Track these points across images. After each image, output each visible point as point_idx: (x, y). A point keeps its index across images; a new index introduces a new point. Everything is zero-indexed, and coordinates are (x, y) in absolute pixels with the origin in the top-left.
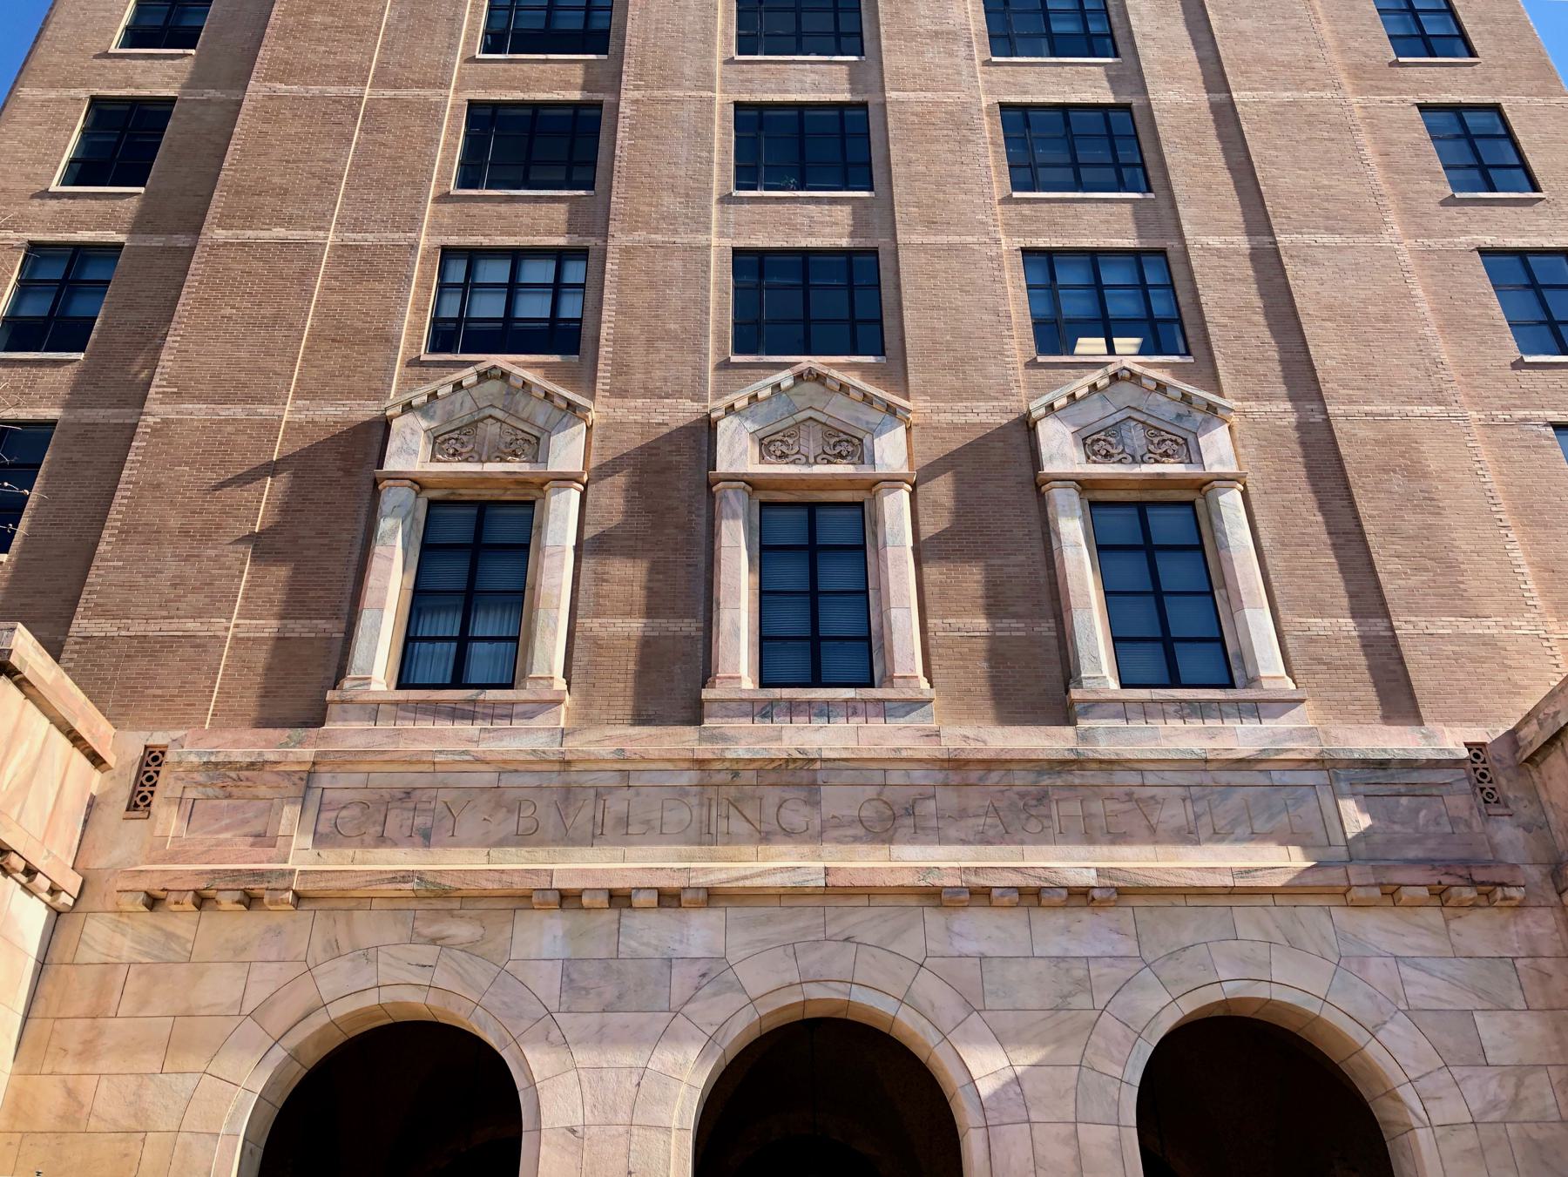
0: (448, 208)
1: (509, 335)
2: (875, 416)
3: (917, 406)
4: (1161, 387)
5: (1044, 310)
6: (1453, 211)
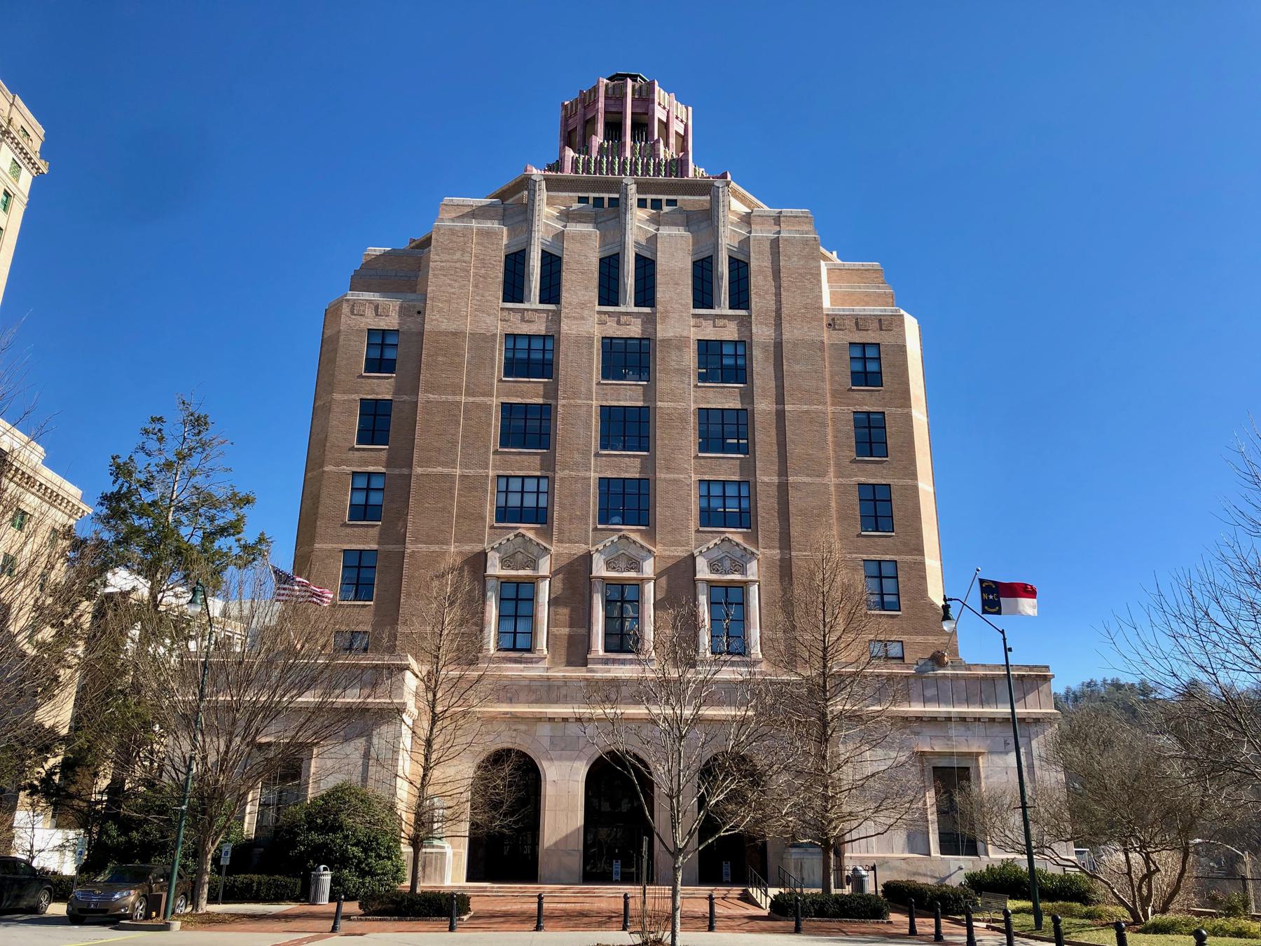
0: (498, 457)
1: (521, 515)
2: (644, 553)
3: (658, 550)
4: (738, 544)
5: (705, 504)
6: (854, 466)
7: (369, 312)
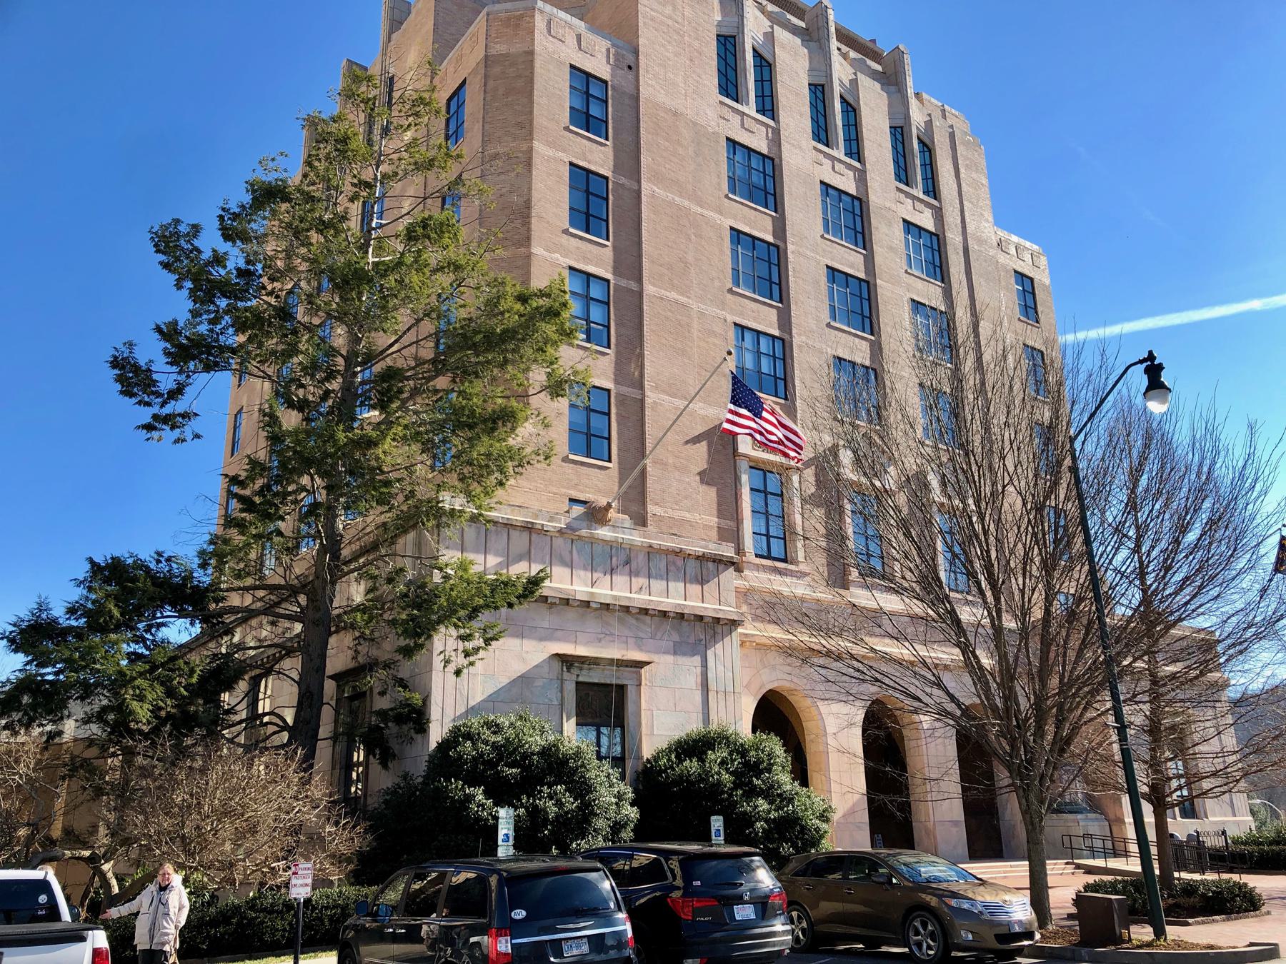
7: (571, 41)
